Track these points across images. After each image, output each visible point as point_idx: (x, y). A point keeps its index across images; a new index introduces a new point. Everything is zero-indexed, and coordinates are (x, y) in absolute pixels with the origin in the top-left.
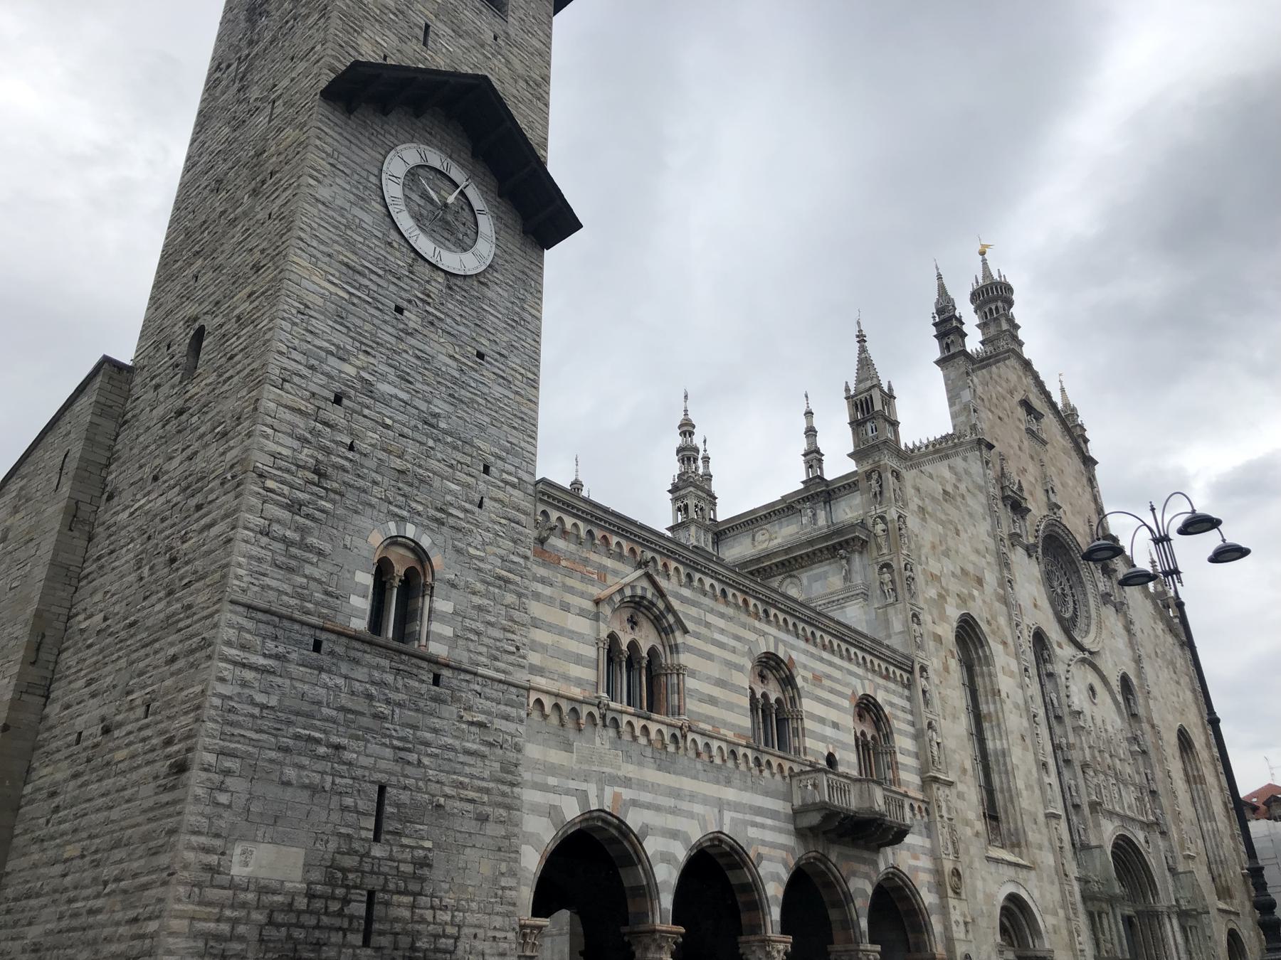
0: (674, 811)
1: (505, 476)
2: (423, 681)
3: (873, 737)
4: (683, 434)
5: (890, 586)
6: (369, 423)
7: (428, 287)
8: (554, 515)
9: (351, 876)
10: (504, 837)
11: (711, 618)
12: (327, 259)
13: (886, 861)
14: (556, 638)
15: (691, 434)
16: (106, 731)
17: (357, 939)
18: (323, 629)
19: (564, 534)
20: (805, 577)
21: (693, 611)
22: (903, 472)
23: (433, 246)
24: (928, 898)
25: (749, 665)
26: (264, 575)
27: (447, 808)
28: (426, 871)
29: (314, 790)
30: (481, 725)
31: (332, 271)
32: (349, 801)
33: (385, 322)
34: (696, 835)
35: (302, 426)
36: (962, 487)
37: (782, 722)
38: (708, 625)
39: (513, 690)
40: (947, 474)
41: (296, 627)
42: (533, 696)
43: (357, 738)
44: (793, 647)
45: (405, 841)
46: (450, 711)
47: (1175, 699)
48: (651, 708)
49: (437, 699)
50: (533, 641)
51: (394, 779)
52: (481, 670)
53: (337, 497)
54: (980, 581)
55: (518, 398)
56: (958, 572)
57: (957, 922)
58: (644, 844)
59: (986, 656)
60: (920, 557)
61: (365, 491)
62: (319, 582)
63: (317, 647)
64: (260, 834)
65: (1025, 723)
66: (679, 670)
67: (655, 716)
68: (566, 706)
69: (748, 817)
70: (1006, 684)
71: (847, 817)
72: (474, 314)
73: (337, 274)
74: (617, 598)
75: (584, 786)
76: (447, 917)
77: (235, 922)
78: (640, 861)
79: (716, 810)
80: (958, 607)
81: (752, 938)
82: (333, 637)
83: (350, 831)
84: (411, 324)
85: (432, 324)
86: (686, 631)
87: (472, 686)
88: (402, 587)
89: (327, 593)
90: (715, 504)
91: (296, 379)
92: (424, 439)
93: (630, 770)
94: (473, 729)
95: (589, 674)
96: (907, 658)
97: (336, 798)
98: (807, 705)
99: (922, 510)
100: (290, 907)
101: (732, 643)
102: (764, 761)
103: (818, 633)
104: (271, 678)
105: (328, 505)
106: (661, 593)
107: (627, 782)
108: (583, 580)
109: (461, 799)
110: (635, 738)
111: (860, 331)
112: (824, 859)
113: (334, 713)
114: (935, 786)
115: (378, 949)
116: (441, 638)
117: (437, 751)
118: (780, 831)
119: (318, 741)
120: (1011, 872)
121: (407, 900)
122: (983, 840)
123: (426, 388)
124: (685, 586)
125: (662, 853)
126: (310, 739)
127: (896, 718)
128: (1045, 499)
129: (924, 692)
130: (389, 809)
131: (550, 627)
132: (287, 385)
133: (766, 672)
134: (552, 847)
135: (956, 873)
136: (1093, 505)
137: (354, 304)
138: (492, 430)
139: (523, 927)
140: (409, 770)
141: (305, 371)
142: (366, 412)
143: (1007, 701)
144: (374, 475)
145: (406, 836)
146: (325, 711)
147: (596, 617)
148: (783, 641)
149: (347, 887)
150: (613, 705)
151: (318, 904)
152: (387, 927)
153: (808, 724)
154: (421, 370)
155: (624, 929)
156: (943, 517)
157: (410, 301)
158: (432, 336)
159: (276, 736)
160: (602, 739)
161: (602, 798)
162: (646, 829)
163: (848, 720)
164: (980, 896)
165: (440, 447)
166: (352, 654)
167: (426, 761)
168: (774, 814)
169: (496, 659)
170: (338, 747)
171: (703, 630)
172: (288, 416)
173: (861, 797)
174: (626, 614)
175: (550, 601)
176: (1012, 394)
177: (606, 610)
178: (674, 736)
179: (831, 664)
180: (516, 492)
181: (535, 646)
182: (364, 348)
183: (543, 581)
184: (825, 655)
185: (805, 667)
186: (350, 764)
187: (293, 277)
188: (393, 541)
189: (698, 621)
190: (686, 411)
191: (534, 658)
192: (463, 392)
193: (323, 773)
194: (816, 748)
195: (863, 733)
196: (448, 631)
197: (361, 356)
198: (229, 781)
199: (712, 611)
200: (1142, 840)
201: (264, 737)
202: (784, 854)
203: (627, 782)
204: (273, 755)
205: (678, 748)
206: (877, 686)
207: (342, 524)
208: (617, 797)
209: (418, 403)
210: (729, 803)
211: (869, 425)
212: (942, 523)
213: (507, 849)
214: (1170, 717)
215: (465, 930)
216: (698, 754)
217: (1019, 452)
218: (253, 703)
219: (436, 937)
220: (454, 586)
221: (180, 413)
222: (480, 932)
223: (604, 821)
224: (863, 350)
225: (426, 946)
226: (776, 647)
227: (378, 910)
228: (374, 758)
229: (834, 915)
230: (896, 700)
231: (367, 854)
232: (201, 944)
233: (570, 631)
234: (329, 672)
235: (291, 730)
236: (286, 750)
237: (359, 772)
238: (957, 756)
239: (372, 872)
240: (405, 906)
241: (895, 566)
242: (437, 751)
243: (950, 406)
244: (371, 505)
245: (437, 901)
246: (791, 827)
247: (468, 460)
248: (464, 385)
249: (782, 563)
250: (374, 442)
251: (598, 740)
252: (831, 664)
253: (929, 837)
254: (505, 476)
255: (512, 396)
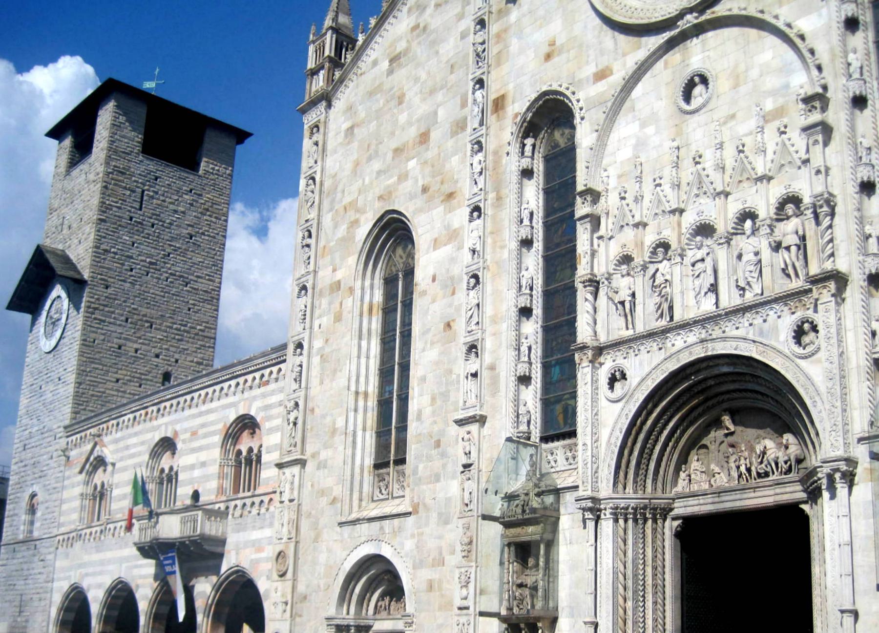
21: (121, 444)
38: (127, 448)
160: (78, 545)
199: (130, 436)
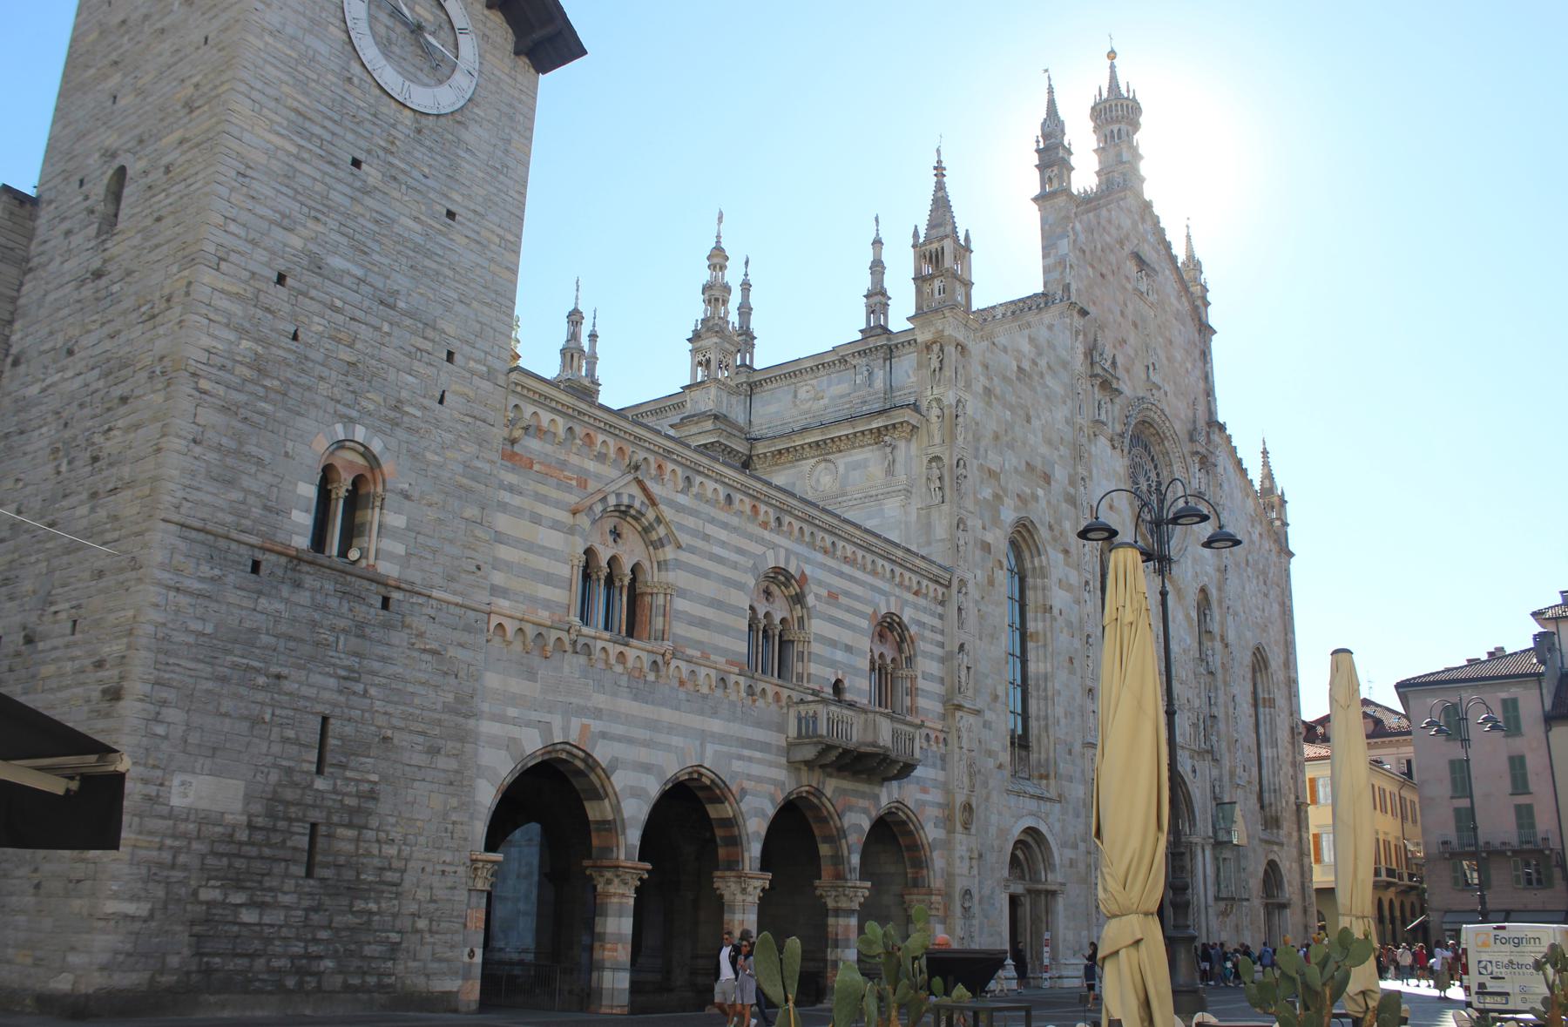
0: (647, 744)
1: (472, 364)
2: (371, 606)
3: (893, 660)
4: (712, 267)
5: (938, 484)
6: (315, 307)
7: (393, 132)
8: (528, 409)
9: (293, 809)
10: (457, 772)
11: (710, 529)
12: (272, 104)
13: (890, 794)
14: (524, 554)
15: (722, 268)
16: (29, 640)
17: (302, 872)
18: (264, 549)
19: (540, 432)
20: (842, 461)
21: (690, 522)
22: (970, 345)
23: (401, 79)
24: (931, 832)
25: (752, 582)
26: (198, 489)
27: (396, 741)
28: (371, 805)
29: (256, 721)
30: (434, 652)
31: (279, 119)
32: (290, 734)
33: (339, 180)
34: (673, 767)
35: (240, 313)
36: (1043, 363)
37: (784, 644)
38: (706, 538)
39: (471, 614)
40: (1026, 347)
41: (234, 546)
42: (495, 620)
43: (300, 667)
44: (807, 561)
45: (349, 774)
46: (399, 638)
47: (1258, 613)
48: (631, 632)
49: (387, 626)
50: (495, 559)
51: (338, 711)
52: (435, 593)
53: (279, 397)
54: (1047, 478)
55: (493, 267)
56: (1023, 467)
57: (962, 858)
58: (613, 779)
59: (1042, 568)
60: (977, 449)
61: (309, 389)
62: (258, 495)
63: (256, 567)
64: (198, 766)
65: (1077, 643)
66: (670, 591)
67: (634, 642)
68: (530, 631)
69: (733, 750)
70: (1059, 598)
71: (846, 752)
72: (447, 163)
73: (285, 123)
74: (598, 508)
75: (547, 718)
76: (391, 851)
77: (176, 851)
78: (607, 795)
79: (698, 743)
80: (1016, 509)
81: (728, 873)
82: (273, 557)
83: (291, 764)
84: (371, 181)
85: (395, 179)
86: (679, 547)
87: (425, 610)
88: (345, 502)
89: (265, 508)
90: (753, 346)
91: (233, 257)
92: (377, 322)
93: (600, 700)
94: (426, 657)
95: (558, 595)
96: (945, 569)
97: (275, 730)
98: (816, 626)
99: (988, 391)
100: (230, 838)
101: (734, 557)
102: (758, 690)
103: (840, 544)
104: (206, 602)
105: (268, 407)
106: (653, 503)
107: (598, 713)
108: (558, 487)
109: (411, 732)
110: (610, 667)
111: (939, 162)
112: (819, 793)
113: (273, 640)
114: (958, 714)
115: (323, 880)
116: (391, 557)
117: (384, 681)
118: (770, 764)
119: (258, 670)
120: (1032, 805)
121: (351, 833)
122: (1007, 772)
123: (383, 260)
124: (682, 492)
125: (632, 788)
126: (248, 668)
127: (923, 638)
128: (1144, 377)
129: (959, 609)
130: (332, 742)
131: (516, 543)
132: (223, 266)
133: (774, 588)
134: (509, 780)
135: (968, 808)
136: (1202, 384)
137: (303, 160)
138: (459, 308)
139: (474, 861)
140: (355, 700)
141: (247, 248)
142: (313, 293)
143: (1060, 619)
144: (319, 368)
145: (352, 770)
146: (265, 639)
147: (571, 531)
148: (797, 555)
149: (290, 820)
150: (585, 630)
151: (259, 836)
152: (331, 859)
153: (816, 648)
154: (378, 237)
155: (586, 863)
156: (1013, 400)
157: (369, 152)
158: (396, 194)
159: (213, 665)
160: (572, 665)
161: (565, 730)
162: (615, 763)
163: (865, 643)
164: (993, 830)
165: (396, 332)
166: (297, 575)
167: (373, 691)
168: (765, 747)
169: (451, 579)
170: (278, 677)
171: (699, 543)
172: (224, 303)
173: (865, 730)
174: (609, 524)
175: (518, 512)
176: (1121, 243)
177: (584, 521)
178: (655, 662)
179: (852, 579)
180: (486, 385)
181: (497, 564)
182: (313, 213)
183: (511, 489)
184: (846, 569)
185: (820, 583)
186: (291, 694)
187: (236, 131)
188: (340, 445)
189: (695, 533)
190: (719, 237)
191: (498, 578)
192: (427, 262)
193: (262, 704)
194: (820, 673)
195: (881, 656)
196: (400, 549)
197: (310, 224)
198: (164, 711)
199: (712, 521)
200: (1189, 769)
201: (201, 666)
202: (772, 788)
203: (598, 713)
204: (209, 685)
205: (658, 677)
206: (905, 603)
207: (283, 428)
208: (585, 728)
209: (372, 278)
210: (713, 735)
211: (937, 283)
212: (1011, 408)
213: (458, 782)
214: (1249, 634)
215: (410, 865)
216: (682, 683)
217: (1120, 319)
218: (187, 630)
219: (382, 869)
220: (407, 497)
221: (98, 275)
222: (429, 869)
223: (569, 753)
224: (940, 186)
225: (370, 878)
226: (787, 561)
227: (321, 843)
228: (320, 687)
229: (824, 850)
230: (926, 619)
231: (310, 786)
232: (144, 871)
233: (540, 547)
234: (269, 595)
235: (229, 658)
236: (224, 679)
237: (302, 703)
238: (989, 681)
239: (314, 806)
240: (350, 840)
241: (946, 461)
242: (384, 681)
243: (1044, 257)
244: (316, 406)
245: (382, 835)
246: (784, 760)
247: (428, 346)
248: (429, 254)
249: (817, 443)
250: (321, 328)
251: (566, 668)
252: (852, 579)
253: (943, 769)
254: (472, 364)
255: (486, 264)
